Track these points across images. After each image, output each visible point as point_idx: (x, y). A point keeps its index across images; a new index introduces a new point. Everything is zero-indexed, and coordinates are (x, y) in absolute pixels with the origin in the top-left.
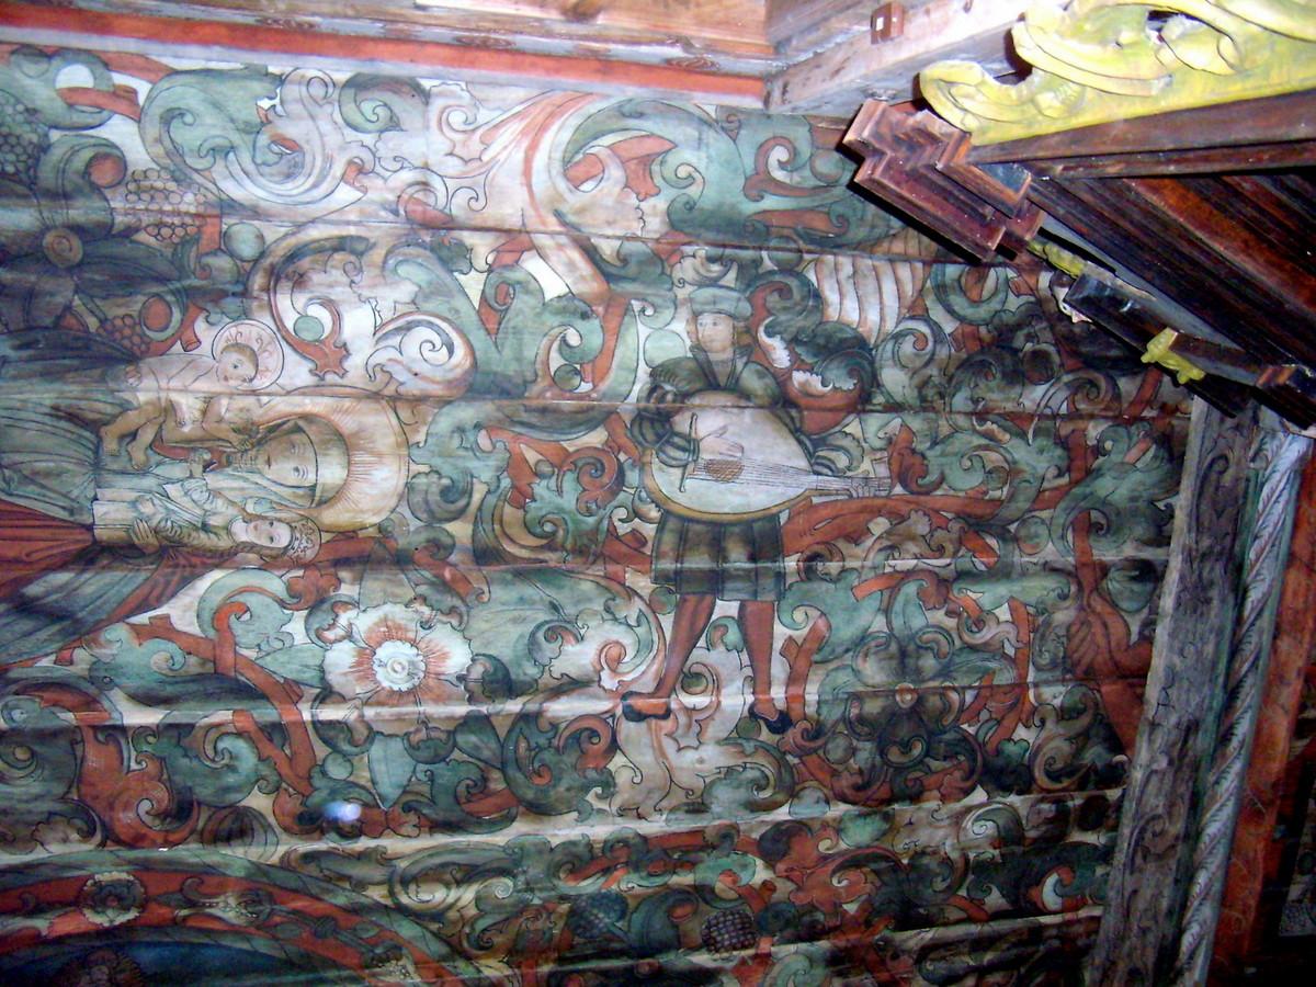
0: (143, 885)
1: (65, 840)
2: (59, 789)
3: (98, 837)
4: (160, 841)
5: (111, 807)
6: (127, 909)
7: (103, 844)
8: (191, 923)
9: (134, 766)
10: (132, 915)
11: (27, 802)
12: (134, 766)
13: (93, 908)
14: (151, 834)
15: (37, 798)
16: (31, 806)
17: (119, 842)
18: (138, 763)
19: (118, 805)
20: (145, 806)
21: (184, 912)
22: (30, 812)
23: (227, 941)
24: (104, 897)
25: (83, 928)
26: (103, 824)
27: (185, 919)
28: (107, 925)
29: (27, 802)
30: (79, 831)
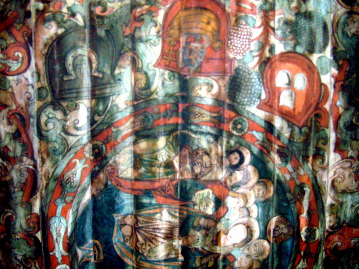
0: (314, 242)
1: (330, 222)
2: (347, 221)
3: (330, 230)
4: (328, 247)
5: (340, 234)
6: (306, 237)
7: (328, 231)
8: (298, 255)
9: (352, 241)
10: (304, 239)
11: (345, 211)
12: (352, 241)
13: (308, 229)
14: (330, 245)
15: (345, 215)
16: (343, 213)
17: (328, 236)
18: (353, 242)
19: (341, 237)
20: (339, 244)
21: (302, 253)
22: (341, 213)
23: (290, 265)
24: (311, 232)
25: (301, 226)
26: (335, 232)
27: (301, 254)
28: (301, 232)
29: (344, 212)
30: (333, 225)
